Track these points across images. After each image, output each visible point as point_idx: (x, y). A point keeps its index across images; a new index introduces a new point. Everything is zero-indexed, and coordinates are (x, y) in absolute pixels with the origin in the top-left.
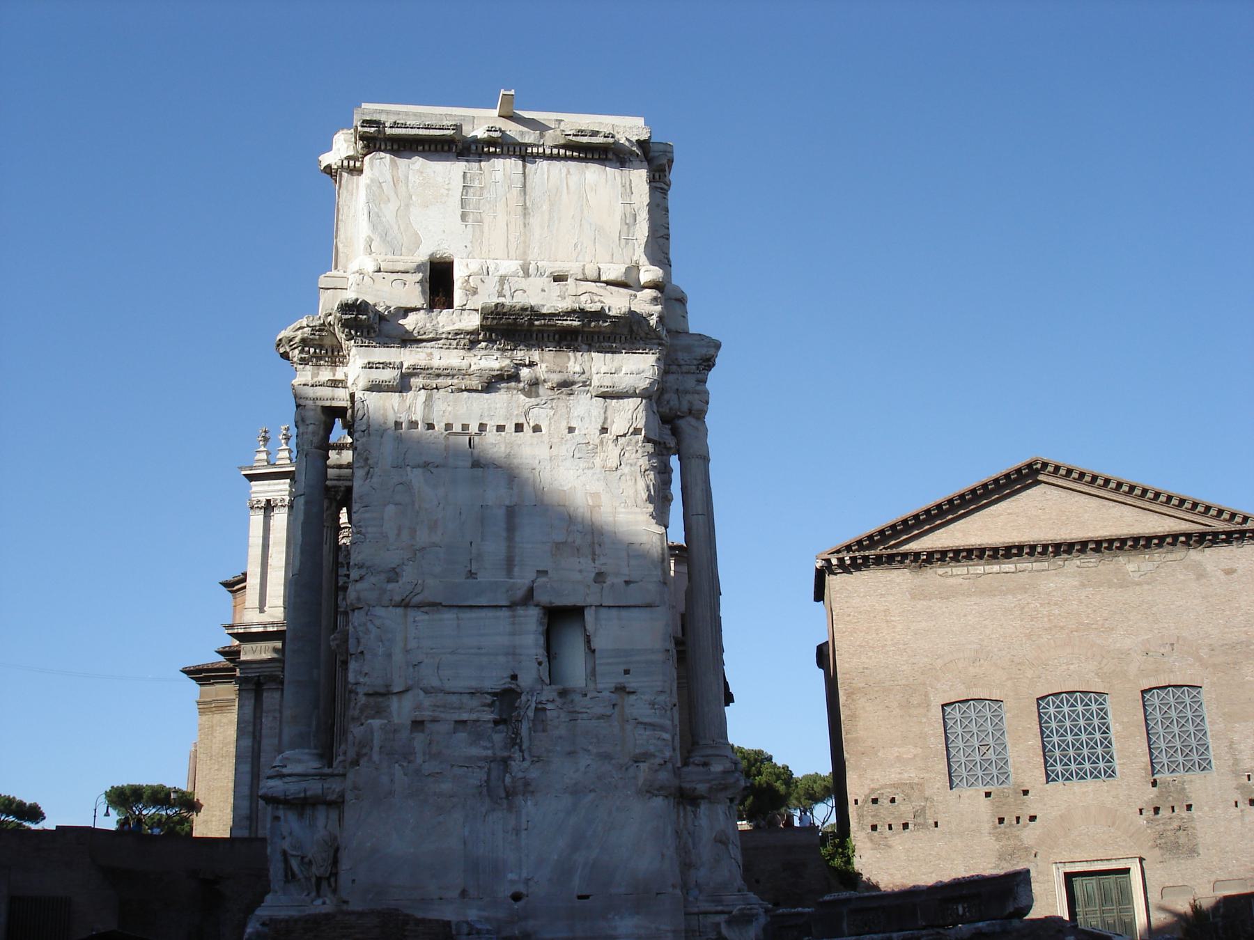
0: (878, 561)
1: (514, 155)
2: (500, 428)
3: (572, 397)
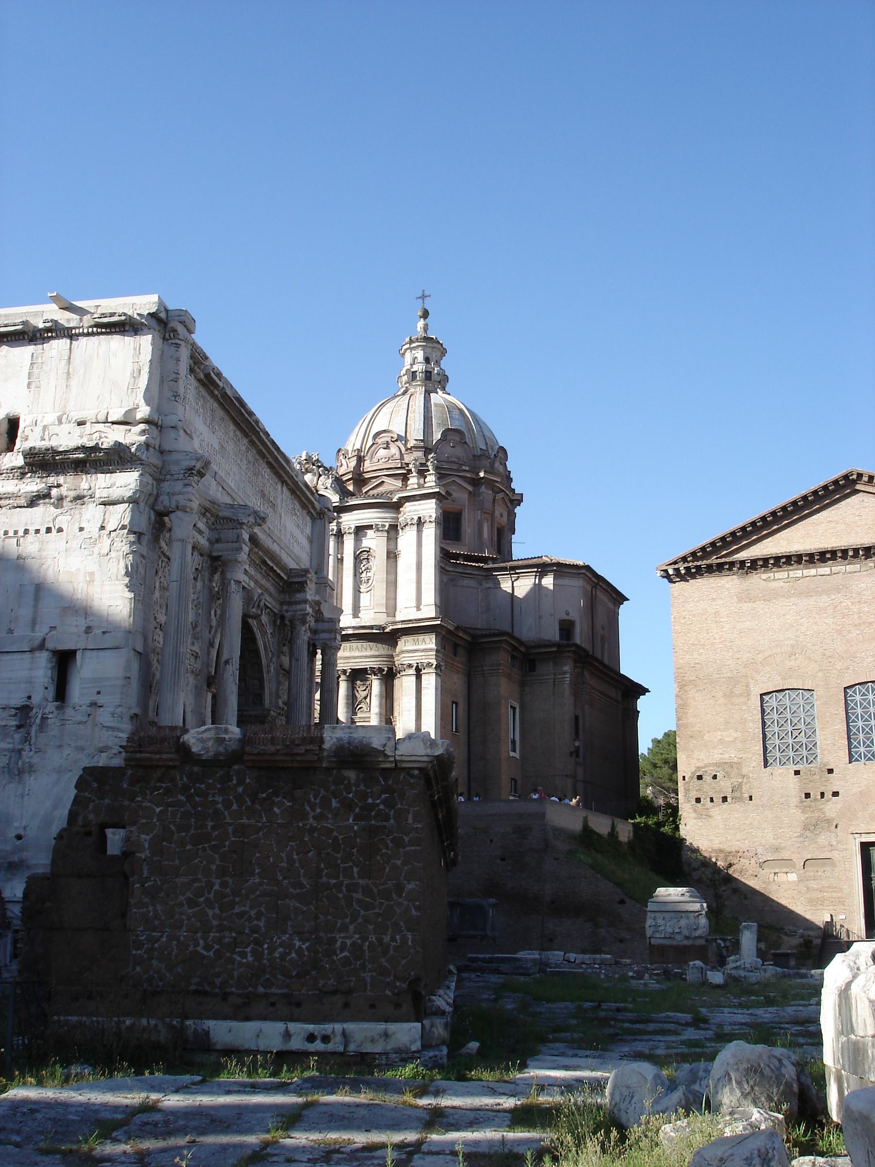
0: (710, 569)
1: (65, 336)
2: (37, 531)
3: (84, 506)
